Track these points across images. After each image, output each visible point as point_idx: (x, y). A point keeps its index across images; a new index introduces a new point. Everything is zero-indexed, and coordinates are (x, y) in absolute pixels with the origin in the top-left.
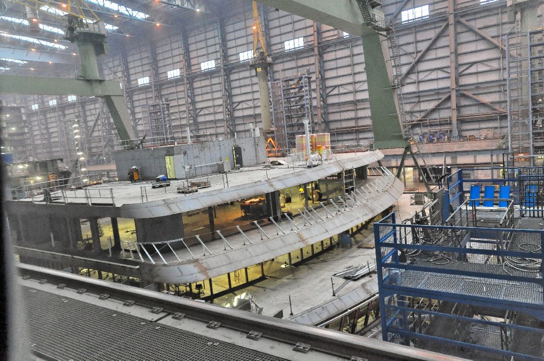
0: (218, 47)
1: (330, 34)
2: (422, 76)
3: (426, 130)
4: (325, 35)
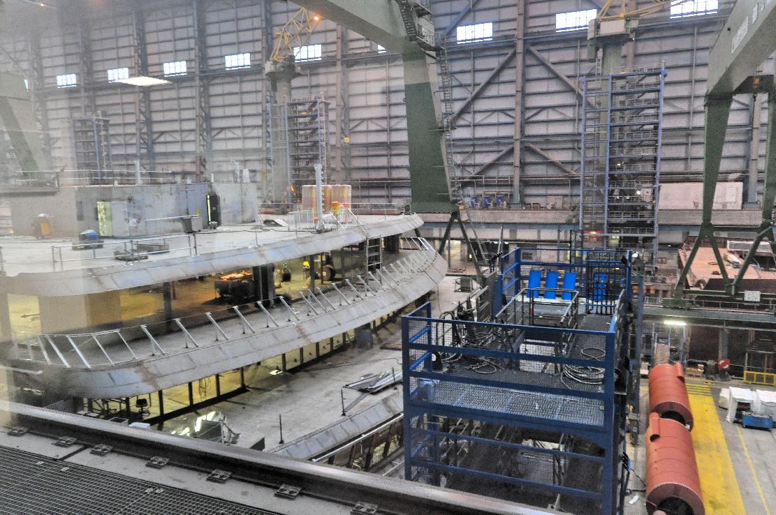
0: (192, 42)
1: (360, 45)
2: (479, 118)
3: (480, 191)
4: (352, 45)
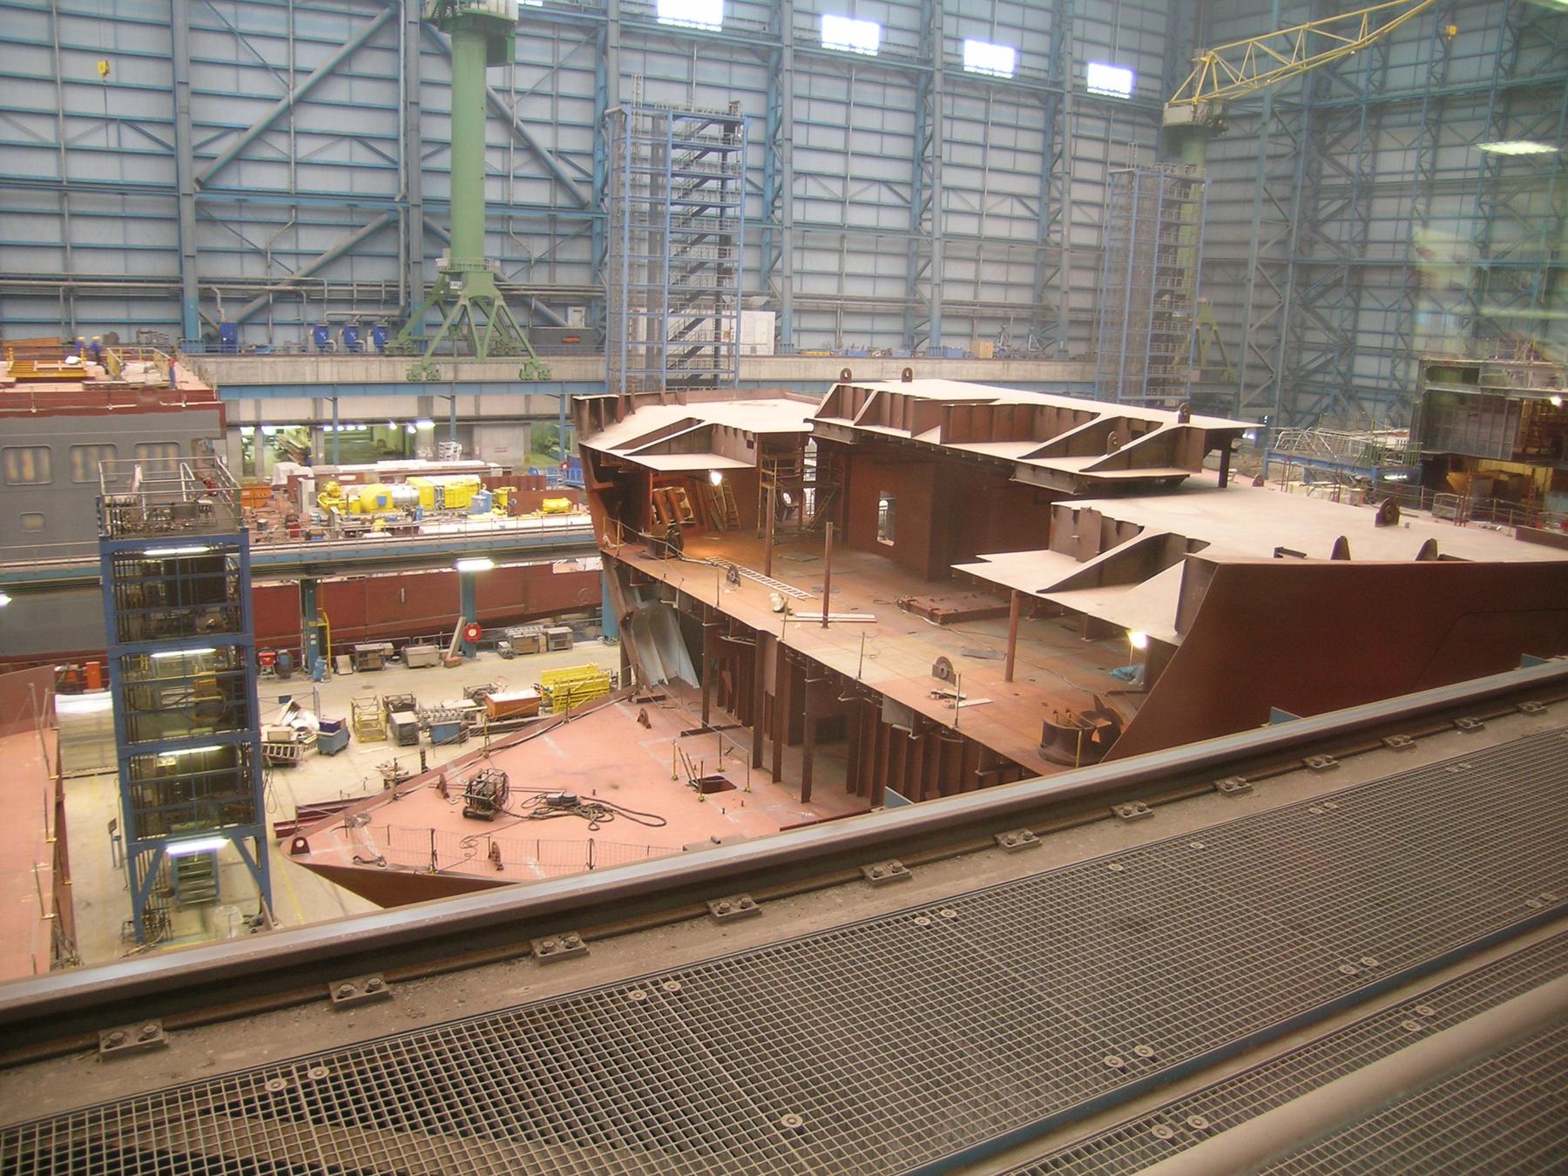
2: (306, 148)
